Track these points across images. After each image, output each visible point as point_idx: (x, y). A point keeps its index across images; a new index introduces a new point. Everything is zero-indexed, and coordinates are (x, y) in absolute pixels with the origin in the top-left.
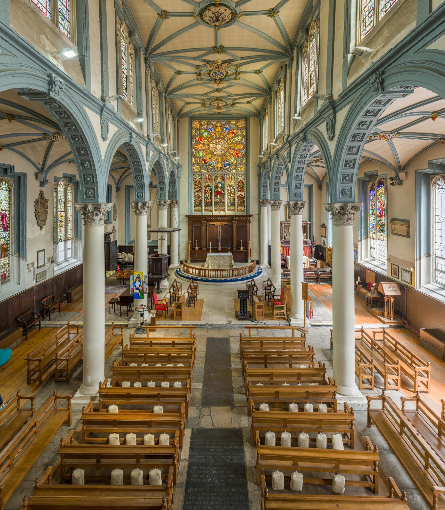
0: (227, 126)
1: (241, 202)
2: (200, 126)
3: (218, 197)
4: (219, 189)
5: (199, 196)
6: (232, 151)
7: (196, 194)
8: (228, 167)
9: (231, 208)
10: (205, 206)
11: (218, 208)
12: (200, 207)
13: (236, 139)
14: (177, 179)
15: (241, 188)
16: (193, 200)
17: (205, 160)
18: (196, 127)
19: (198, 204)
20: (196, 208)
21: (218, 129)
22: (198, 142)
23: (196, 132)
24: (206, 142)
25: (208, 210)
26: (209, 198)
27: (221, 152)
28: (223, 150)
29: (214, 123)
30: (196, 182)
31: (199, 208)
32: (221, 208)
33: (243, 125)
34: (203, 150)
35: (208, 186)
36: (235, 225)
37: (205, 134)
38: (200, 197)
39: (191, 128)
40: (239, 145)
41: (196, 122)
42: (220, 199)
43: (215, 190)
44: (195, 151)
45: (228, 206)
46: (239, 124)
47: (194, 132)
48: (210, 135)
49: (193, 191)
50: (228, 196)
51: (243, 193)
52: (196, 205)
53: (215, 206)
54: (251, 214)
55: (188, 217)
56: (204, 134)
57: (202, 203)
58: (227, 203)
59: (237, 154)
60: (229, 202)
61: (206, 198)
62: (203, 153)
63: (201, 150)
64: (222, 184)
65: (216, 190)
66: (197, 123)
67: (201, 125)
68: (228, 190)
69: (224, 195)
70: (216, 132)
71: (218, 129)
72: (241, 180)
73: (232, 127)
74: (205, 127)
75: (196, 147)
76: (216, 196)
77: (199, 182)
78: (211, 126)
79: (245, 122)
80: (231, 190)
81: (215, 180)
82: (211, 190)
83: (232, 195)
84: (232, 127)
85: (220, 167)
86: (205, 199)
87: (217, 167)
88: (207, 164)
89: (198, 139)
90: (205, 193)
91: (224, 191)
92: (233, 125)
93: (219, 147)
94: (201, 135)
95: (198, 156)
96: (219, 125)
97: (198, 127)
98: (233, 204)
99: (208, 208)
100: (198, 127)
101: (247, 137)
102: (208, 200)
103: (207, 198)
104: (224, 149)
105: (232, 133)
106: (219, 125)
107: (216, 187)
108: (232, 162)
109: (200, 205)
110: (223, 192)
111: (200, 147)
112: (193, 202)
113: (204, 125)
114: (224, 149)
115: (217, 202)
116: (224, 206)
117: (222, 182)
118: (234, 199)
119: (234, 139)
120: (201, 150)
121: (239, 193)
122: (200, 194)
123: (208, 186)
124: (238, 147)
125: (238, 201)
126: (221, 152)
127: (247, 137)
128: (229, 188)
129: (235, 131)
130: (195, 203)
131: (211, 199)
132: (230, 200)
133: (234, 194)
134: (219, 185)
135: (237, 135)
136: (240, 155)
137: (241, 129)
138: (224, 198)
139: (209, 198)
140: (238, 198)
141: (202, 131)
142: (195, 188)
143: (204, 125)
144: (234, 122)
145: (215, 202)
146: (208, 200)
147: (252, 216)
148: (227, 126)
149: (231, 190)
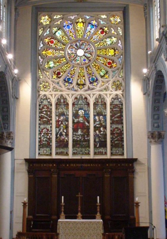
0: (94, 22)
1: (116, 141)
2: (50, 22)
3: (80, 132)
4: (81, 120)
5: (48, 130)
6: (101, 60)
7: (42, 127)
8: (95, 84)
9: (101, 150)
10: (56, 147)
11: (79, 150)
12: (48, 149)
13: (109, 41)
14: (11, 100)
15: (117, 117)
16: (38, 136)
17: (59, 74)
18: (44, 24)
19: (45, 144)
20: (42, 150)
21: (80, 26)
22: (47, 47)
23: (43, 30)
24: (59, 46)
25: (61, 154)
26: (64, 133)
27: (84, 60)
28: (88, 58)
29: (73, 18)
30: (43, 108)
31: (44, 150)
32: (84, 150)
33: (119, 20)
34: (56, 58)
35: (63, 114)
36: (107, 176)
37: (59, 34)
38: (49, 132)
39: (36, 24)
40: (113, 51)
41: (44, 16)
42: (83, 136)
43: (73, 121)
44: (41, 60)
45: (95, 146)
46: (112, 19)
47: (40, 32)
48: (66, 35)
49: (38, 122)
50: (95, 131)
51: (120, 126)
52: (41, 146)
53: (74, 146)
54: (134, 157)
55: (26, 160)
56: (57, 34)
57: (51, 141)
58: (95, 141)
59: (109, 63)
60: (97, 140)
61: (59, 135)
62: (55, 63)
63: (50, 59)
64: (85, 111)
65: (76, 121)
66: (47, 17)
67: (52, 20)
68: (95, 121)
69: (88, 128)
70: (76, 30)
71: (80, 26)
72: (116, 105)
73: (102, 22)
74: (59, 23)
75: (44, 52)
76: (75, 130)
77: (48, 108)
78: (69, 22)
79: (122, 15)
80: (100, 121)
81: (73, 104)
82: (67, 120)
83: (102, 129)
84: (102, 22)
85: (84, 85)
86: (56, 135)
87: (77, 84)
88: (62, 79)
89: (47, 40)
90: (58, 126)
91: (89, 122)
92: (103, 20)
93: (80, 52)
94: (53, 36)
95: (46, 66)
96: (80, 20)
97: (48, 23)
98: (103, 144)
99: (61, 150)
100: (48, 23)
101: (126, 37)
102: (62, 138)
103: (61, 135)
104: (89, 55)
105: (102, 33)
106: (80, 20)
107: (76, 115)
108: (102, 77)
109: (49, 145)
110: (87, 123)
111: (50, 53)
112: (37, 140)
113: (57, 20)
114: (89, 55)
115: (77, 141)
116: (89, 146)
117: (86, 107)
118: (106, 135)
119: (105, 42)
120: (50, 59)
121: (114, 126)
122: (48, 127)
123: (63, 114)
124: (111, 52)
125: (112, 139)
126: (84, 60)
127: (126, 37)
128: (97, 118)
129: (106, 29)
130: (40, 142)
131: (67, 135)
132: (99, 137)
133: (105, 127)
134: (81, 112)
135: (110, 34)
136: (114, 65)
137: (115, 27)
138: (88, 135)
139: (64, 133)
140: (112, 133)
141: (55, 29)
142: (41, 118)
143: (57, 20)
144: (104, 17)
145: (74, 141)
146: (62, 138)
147: (136, 160)
148: (94, 22)
149: (100, 121)
